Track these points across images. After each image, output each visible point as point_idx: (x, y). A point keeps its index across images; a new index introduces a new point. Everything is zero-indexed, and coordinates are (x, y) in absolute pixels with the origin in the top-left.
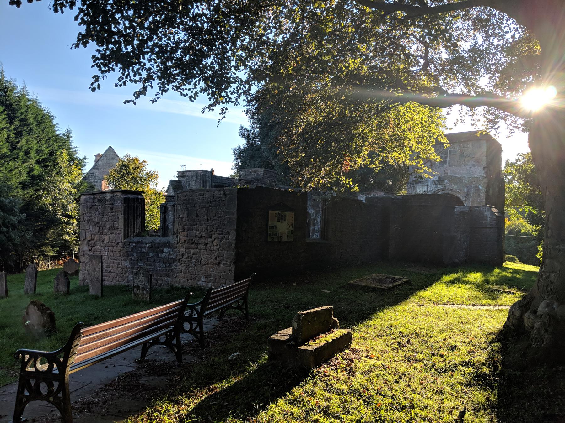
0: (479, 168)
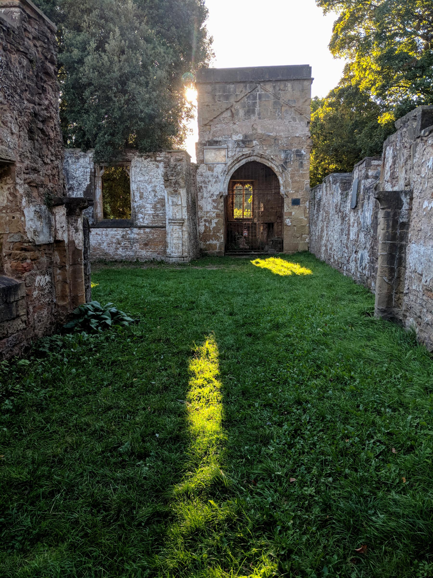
0: (302, 123)
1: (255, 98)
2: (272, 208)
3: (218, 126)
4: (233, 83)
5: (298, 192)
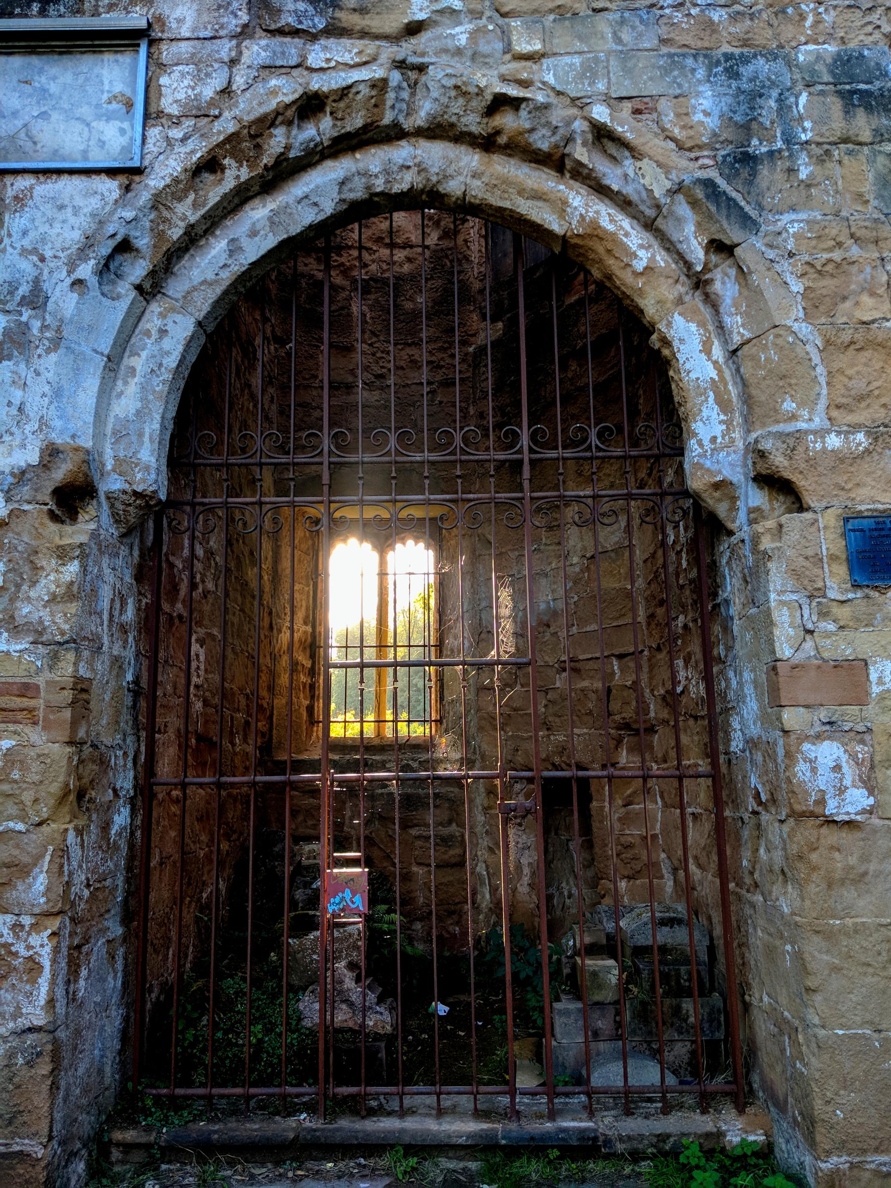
2: (575, 668)
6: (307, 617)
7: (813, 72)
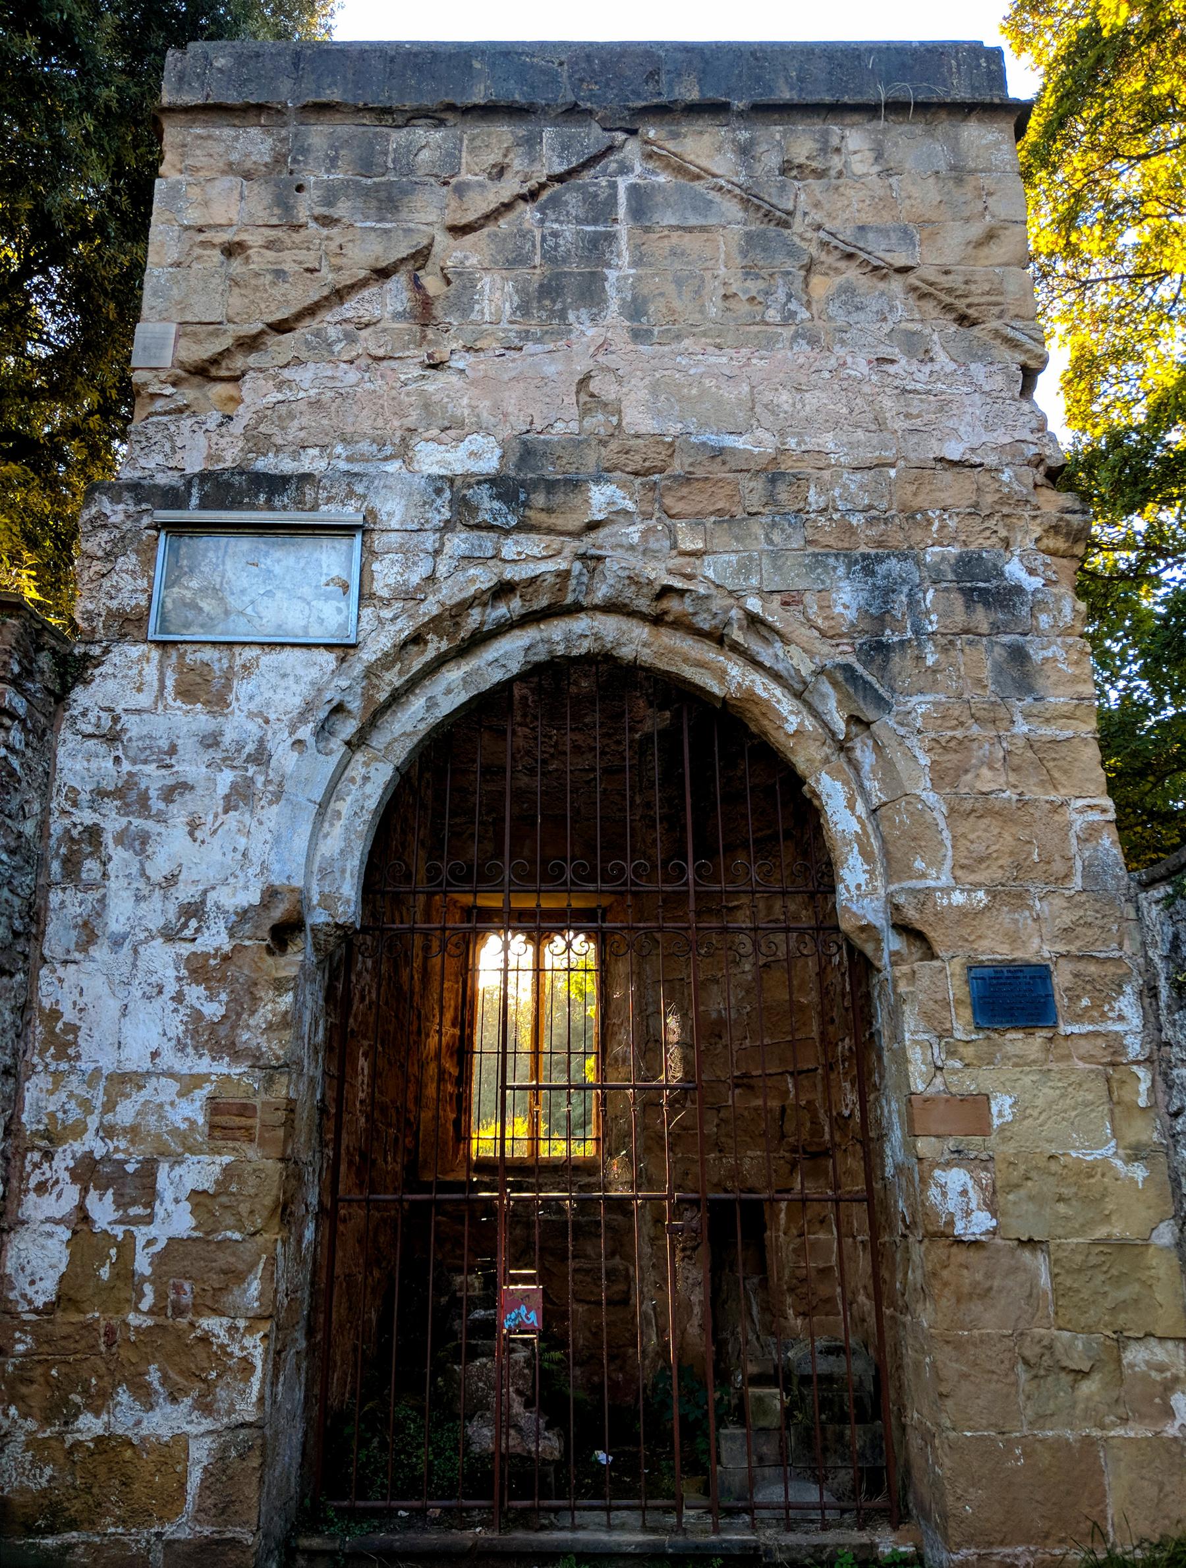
0: (977, 370)
1: (602, 210)
3: (303, 376)
4: (435, 116)
5: (1019, 899)
6: (456, 1018)
7: (939, 572)
